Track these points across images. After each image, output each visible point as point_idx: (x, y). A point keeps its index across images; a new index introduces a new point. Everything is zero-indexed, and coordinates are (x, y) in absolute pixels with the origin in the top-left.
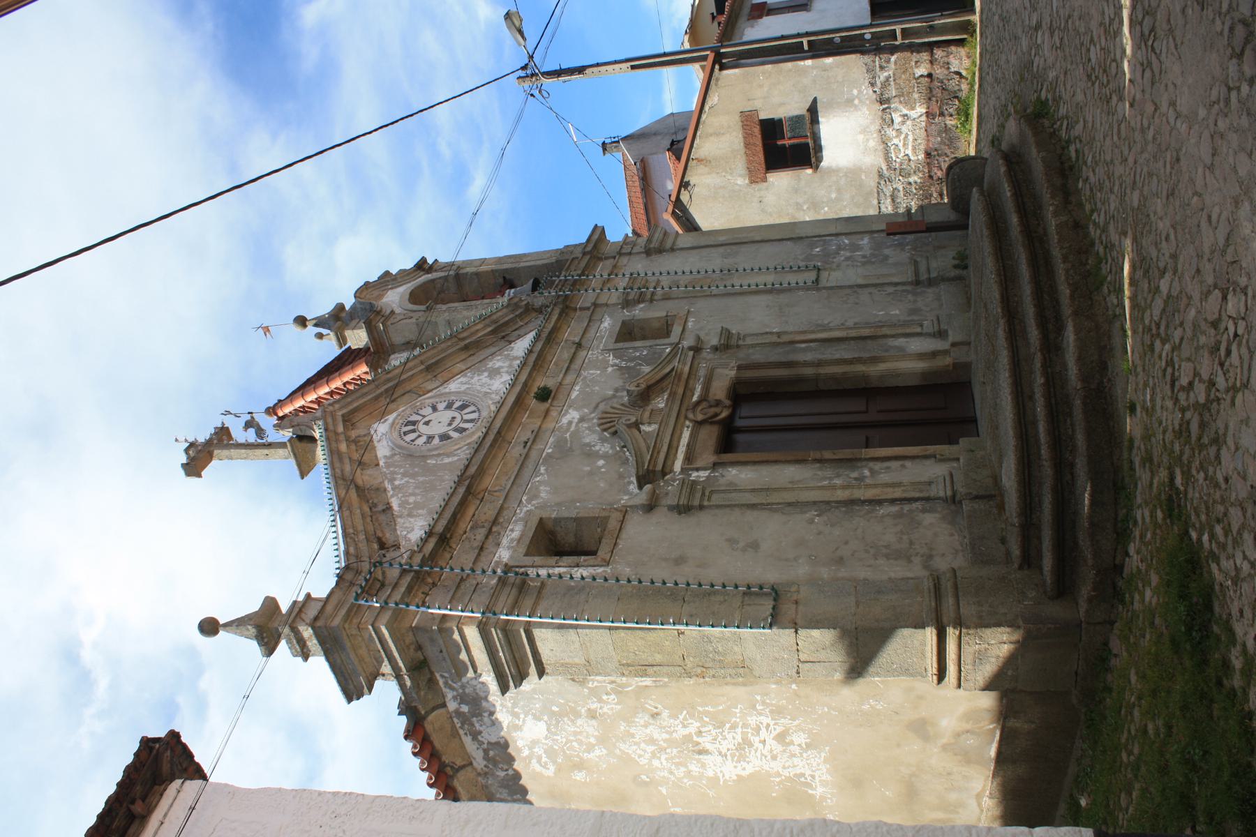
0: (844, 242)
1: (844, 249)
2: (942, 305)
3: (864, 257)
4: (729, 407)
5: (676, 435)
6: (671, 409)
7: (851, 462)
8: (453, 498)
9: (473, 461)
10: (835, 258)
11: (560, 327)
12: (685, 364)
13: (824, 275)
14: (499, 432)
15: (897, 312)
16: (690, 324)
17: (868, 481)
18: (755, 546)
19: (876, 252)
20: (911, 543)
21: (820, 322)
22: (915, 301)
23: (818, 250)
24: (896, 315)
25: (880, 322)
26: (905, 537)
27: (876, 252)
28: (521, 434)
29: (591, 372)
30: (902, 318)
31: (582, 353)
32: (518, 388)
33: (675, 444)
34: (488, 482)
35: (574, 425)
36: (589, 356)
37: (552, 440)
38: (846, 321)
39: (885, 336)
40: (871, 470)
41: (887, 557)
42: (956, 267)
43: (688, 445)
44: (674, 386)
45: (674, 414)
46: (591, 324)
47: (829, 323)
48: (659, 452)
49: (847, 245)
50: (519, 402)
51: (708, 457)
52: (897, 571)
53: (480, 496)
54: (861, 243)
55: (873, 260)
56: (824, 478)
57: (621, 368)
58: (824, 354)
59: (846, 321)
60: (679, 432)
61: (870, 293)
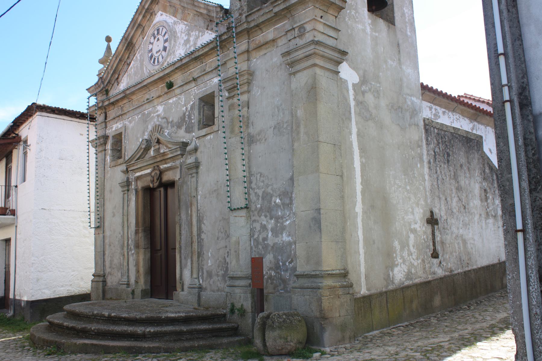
0: (287, 220)
1: (277, 221)
2: (214, 292)
3: (265, 239)
4: (153, 186)
5: (145, 168)
6: (149, 160)
7: (137, 246)
8: (119, 95)
9: (131, 89)
10: (266, 216)
11: (211, 53)
12: (172, 153)
13: (243, 213)
14: (145, 86)
15: (210, 264)
16: (208, 137)
17: (130, 253)
18: (114, 216)
19: (270, 248)
20: (114, 268)
21: (205, 218)
22: (218, 276)
23: (278, 201)
24: (208, 263)
25: (203, 254)
26: (115, 266)
27: (270, 248)
28: (154, 92)
29: (183, 99)
30: (205, 267)
31: (193, 84)
32: (161, 74)
33: (142, 169)
34: (134, 97)
35: (156, 114)
36: (193, 89)
37: (150, 109)
38: (205, 233)
39: (192, 258)
40: (134, 253)
41: (111, 261)
42: (233, 305)
43: (142, 175)
44: (158, 156)
45: (148, 163)
46: (214, 71)
47: (204, 224)
48: (133, 166)
49: (282, 223)
50: (161, 79)
51: (140, 185)
52: (107, 264)
53: (130, 100)
54: (284, 235)
55: (260, 247)
56: (131, 236)
57: (184, 114)
58: (184, 224)
59: (205, 233)
60: (147, 168)
61: (226, 247)
